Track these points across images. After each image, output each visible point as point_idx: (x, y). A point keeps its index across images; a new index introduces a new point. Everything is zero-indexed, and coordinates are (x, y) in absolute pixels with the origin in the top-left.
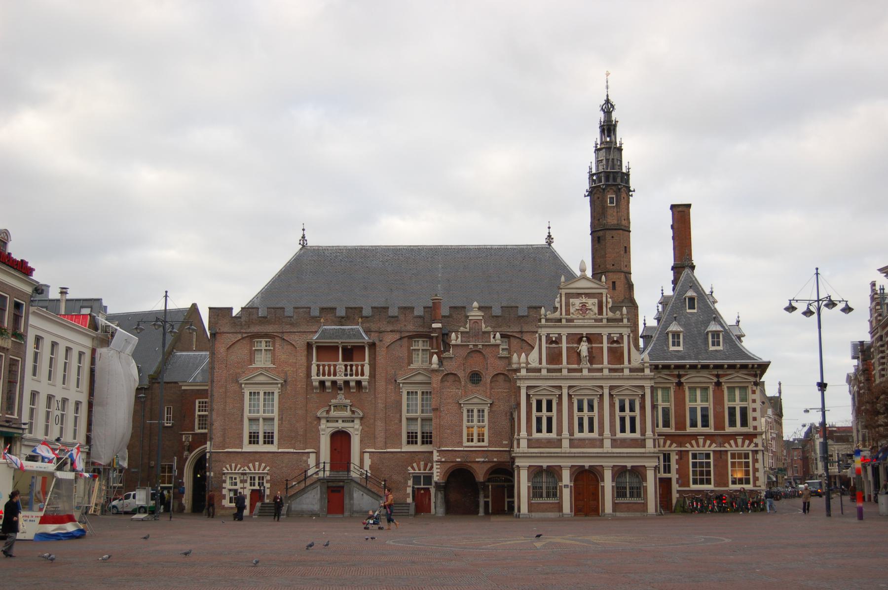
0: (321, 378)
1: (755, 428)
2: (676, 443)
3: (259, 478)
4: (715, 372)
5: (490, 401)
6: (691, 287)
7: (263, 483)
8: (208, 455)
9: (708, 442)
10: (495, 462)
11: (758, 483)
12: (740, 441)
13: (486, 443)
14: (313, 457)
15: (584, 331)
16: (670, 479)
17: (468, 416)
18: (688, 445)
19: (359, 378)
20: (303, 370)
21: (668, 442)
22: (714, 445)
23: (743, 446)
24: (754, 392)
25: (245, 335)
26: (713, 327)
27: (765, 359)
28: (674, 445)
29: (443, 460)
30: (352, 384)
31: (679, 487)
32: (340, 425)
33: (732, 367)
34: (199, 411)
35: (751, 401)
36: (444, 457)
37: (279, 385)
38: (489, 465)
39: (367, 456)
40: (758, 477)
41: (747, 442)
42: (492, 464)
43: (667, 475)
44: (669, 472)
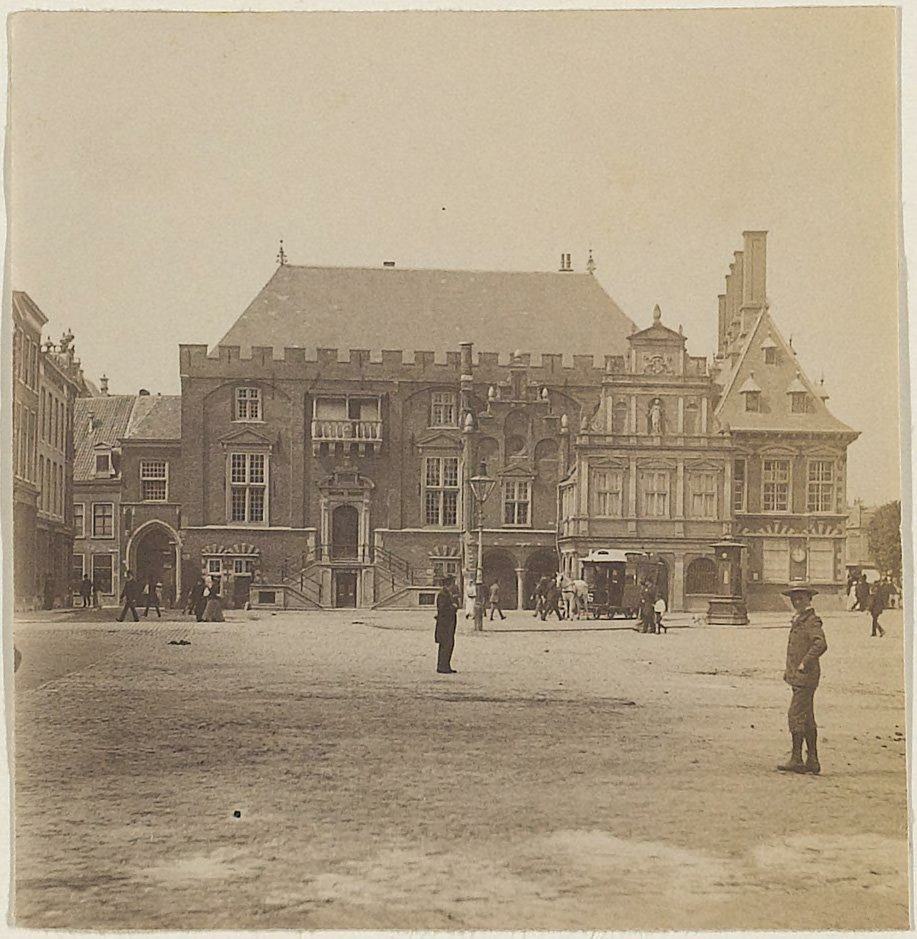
0: (323, 438)
1: (838, 511)
3: (247, 562)
5: (536, 474)
6: (770, 335)
11: (839, 577)
12: (821, 528)
13: (529, 524)
15: (657, 392)
17: (508, 491)
19: (370, 439)
20: (300, 428)
22: (792, 530)
23: (824, 533)
25: (227, 382)
26: (796, 386)
27: (856, 429)
30: (362, 448)
32: (345, 498)
33: (818, 436)
34: (144, 475)
37: (271, 447)
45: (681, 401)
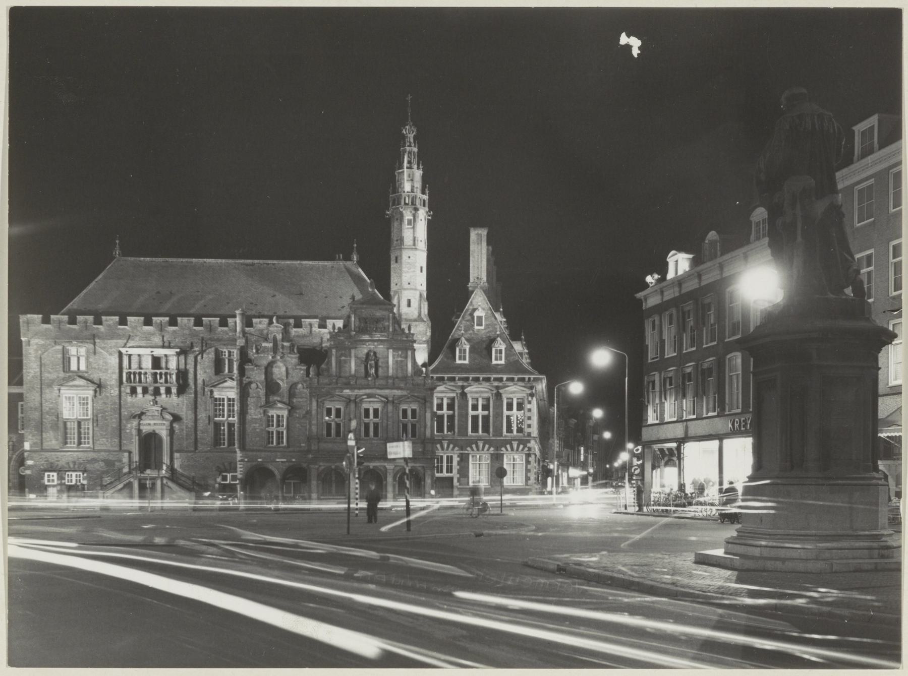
2: (458, 447)
4: (496, 384)
7: (80, 480)
8: (26, 454)
9: (487, 446)
10: (294, 462)
14: (126, 454)
16: (451, 479)
18: (469, 449)
20: (116, 376)
21: (451, 446)
22: (492, 449)
24: (530, 402)
28: (456, 448)
29: (246, 460)
31: (460, 485)
35: (526, 410)
36: (246, 458)
38: (287, 464)
39: (176, 455)
40: (529, 477)
41: (521, 447)
42: (291, 464)
43: (449, 475)
44: (451, 472)
45: (391, 351)
